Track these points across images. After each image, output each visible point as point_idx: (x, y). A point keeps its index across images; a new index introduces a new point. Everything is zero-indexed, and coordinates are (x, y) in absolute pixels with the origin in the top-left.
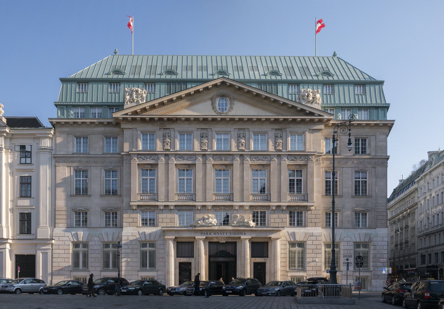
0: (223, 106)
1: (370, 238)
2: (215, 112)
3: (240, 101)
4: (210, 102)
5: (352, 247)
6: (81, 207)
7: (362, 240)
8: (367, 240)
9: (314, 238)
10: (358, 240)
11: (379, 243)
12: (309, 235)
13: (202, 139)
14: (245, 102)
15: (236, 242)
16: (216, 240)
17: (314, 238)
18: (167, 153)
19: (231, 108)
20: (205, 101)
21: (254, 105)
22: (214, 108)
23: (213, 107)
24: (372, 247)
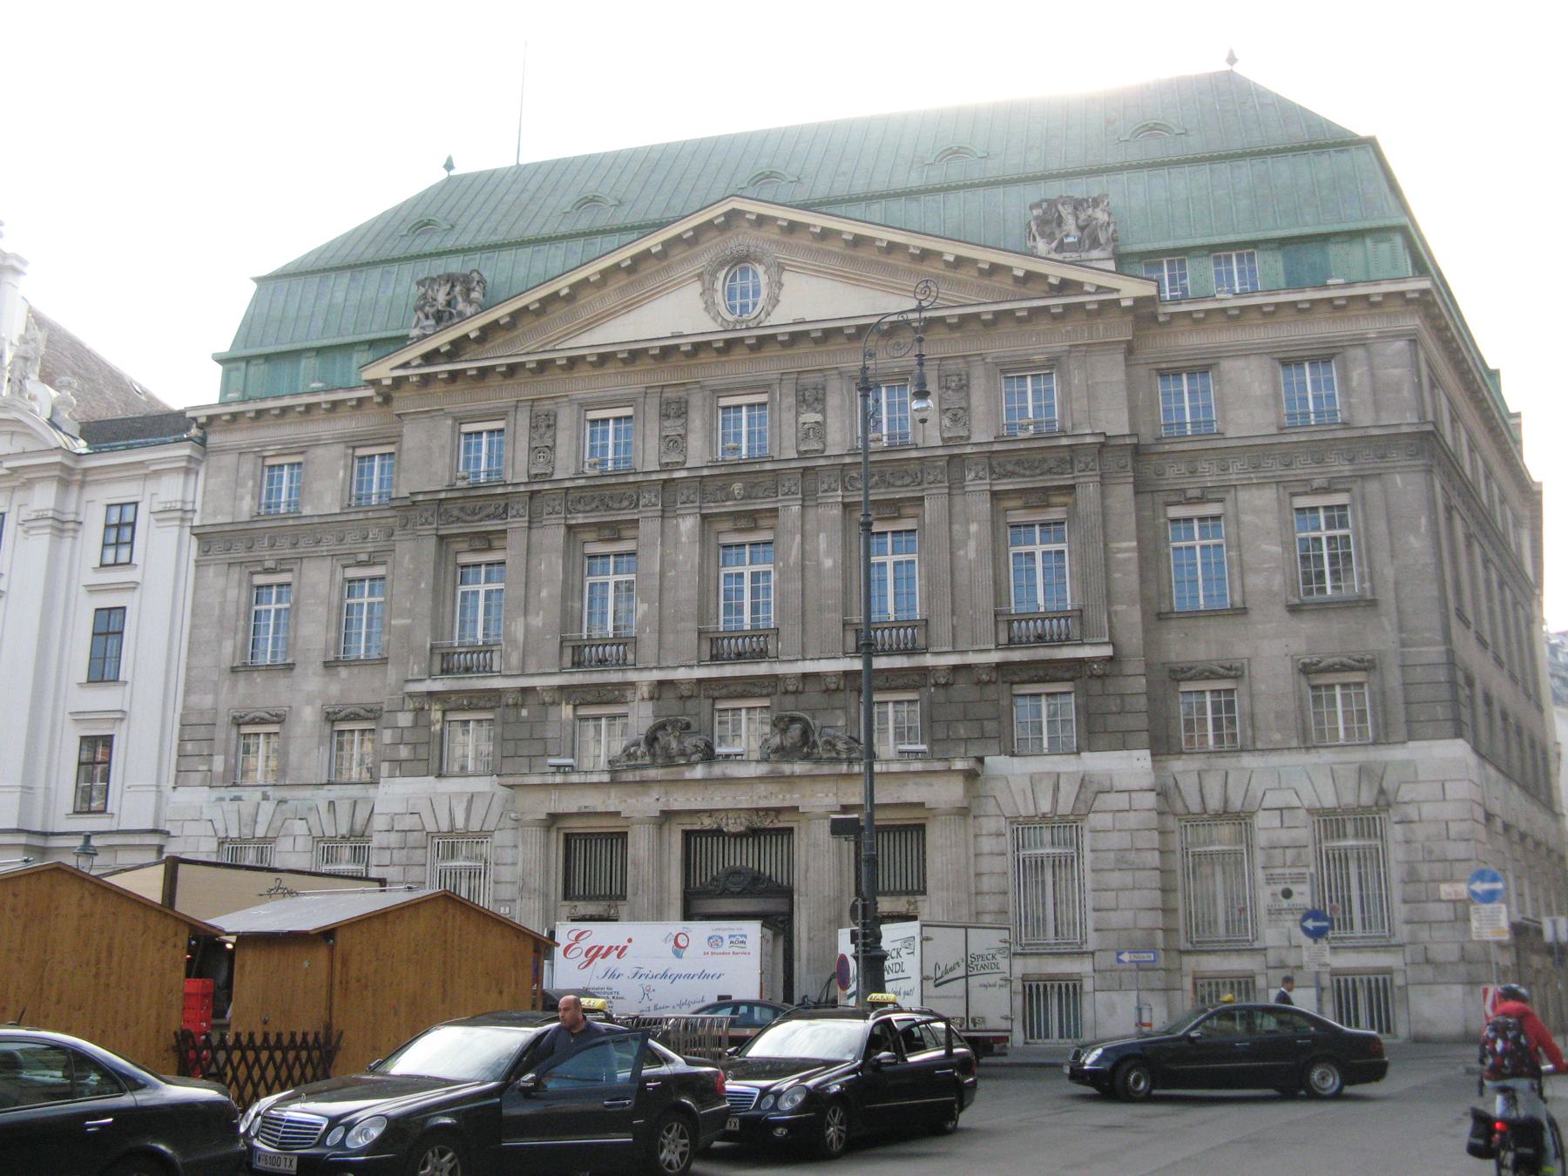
0: (744, 295)
1: (1382, 791)
2: (714, 319)
3: (801, 269)
4: (697, 287)
5: (1303, 834)
6: (258, 710)
7: (1349, 799)
8: (1367, 798)
9: (1121, 801)
10: (1329, 801)
11: (1428, 810)
12: (1095, 787)
13: (666, 424)
14: (817, 272)
15: (791, 830)
16: (707, 823)
17: (1121, 801)
18: (536, 487)
19: (774, 301)
20: (680, 284)
21: (857, 281)
22: (710, 306)
23: (706, 302)
24: (1396, 832)
